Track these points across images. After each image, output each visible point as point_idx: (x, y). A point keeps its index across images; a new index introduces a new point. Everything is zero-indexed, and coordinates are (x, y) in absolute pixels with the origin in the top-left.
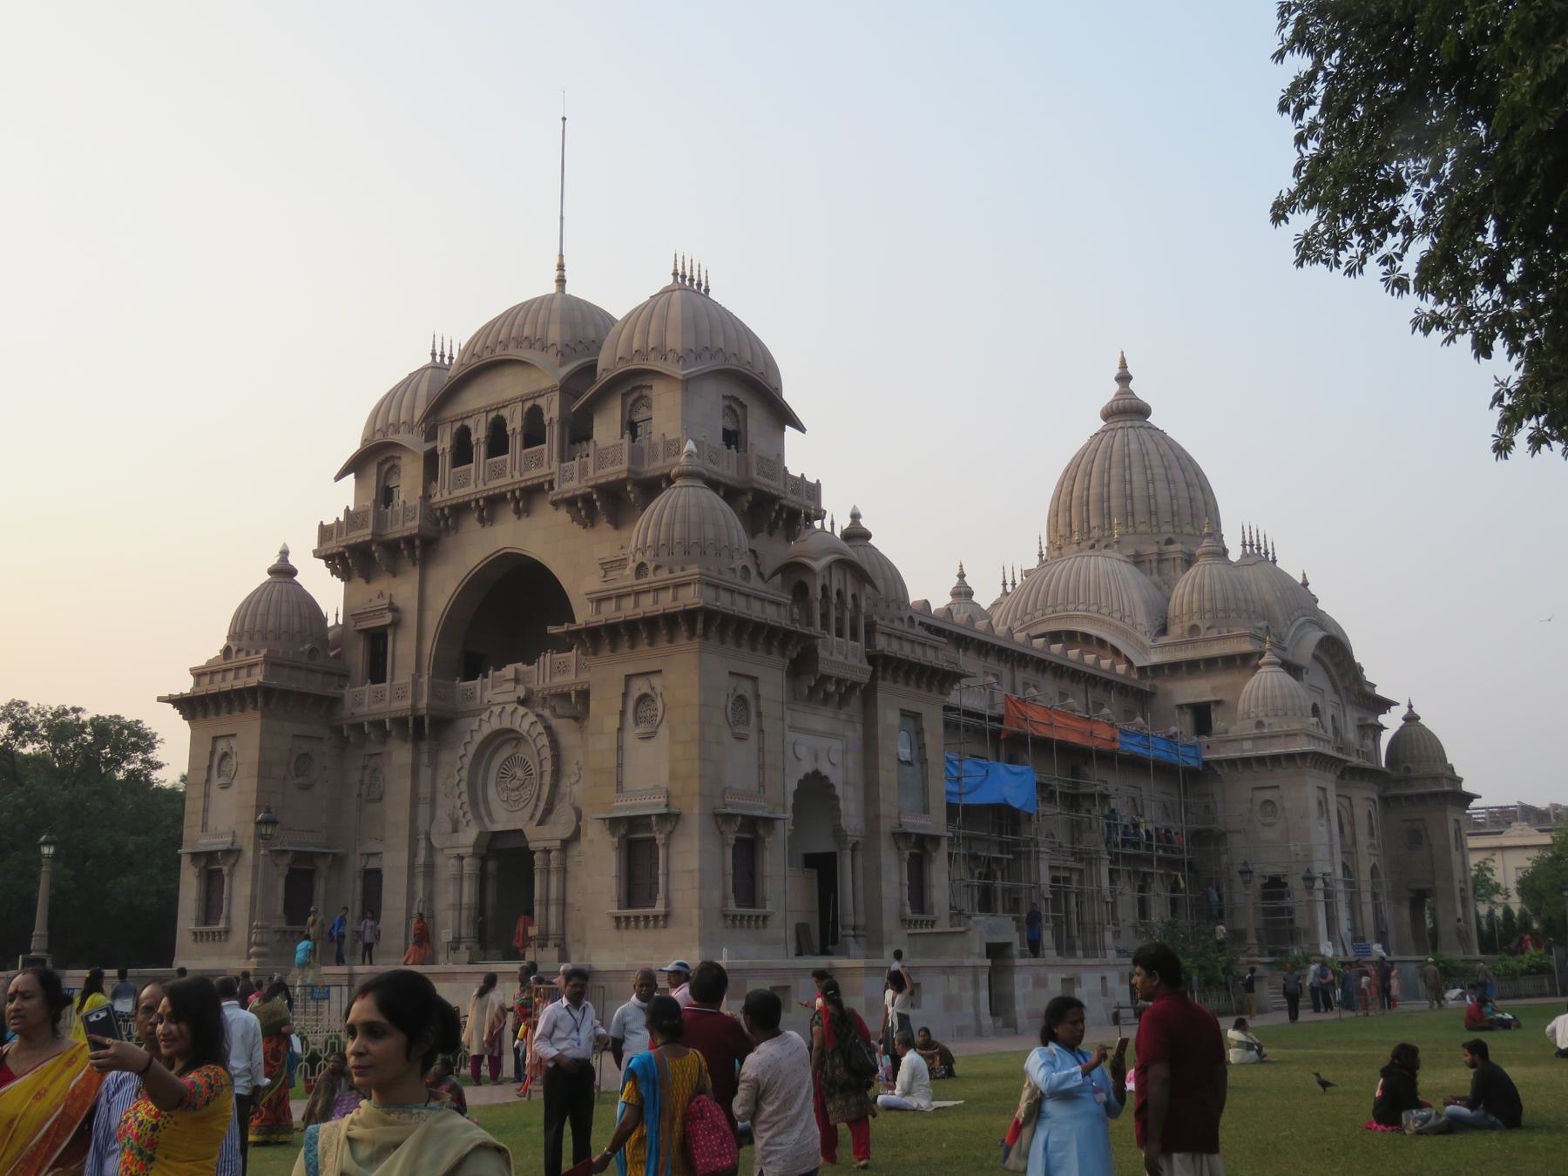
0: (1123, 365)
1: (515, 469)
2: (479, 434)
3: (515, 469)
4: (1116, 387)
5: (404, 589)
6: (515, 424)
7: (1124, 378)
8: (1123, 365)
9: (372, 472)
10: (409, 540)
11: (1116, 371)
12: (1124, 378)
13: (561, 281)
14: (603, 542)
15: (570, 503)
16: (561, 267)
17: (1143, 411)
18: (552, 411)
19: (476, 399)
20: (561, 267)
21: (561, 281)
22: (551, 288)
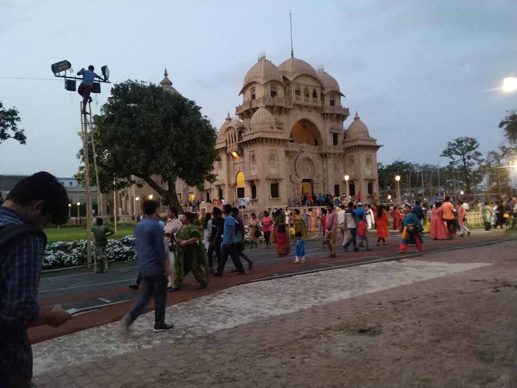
0: (166, 71)
1: (311, 101)
2: (302, 89)
3: (311, 101)
4: (164, 77)
5: (283, 119)
6: (311, 92)
7: (166, 75)
8: (166, 71)
9: (269, 86)
10: (290, 109)
11: (164, 73)
12: (166, 75)
13: (292, 54)
14: (329, 124)
15: (327, 114)
16: (292, 51)
17: (171, 84)
18: (319, 92)
19: (301, 81)
20: (292, 51)
21: (292, 54)
22: (290, 56)
